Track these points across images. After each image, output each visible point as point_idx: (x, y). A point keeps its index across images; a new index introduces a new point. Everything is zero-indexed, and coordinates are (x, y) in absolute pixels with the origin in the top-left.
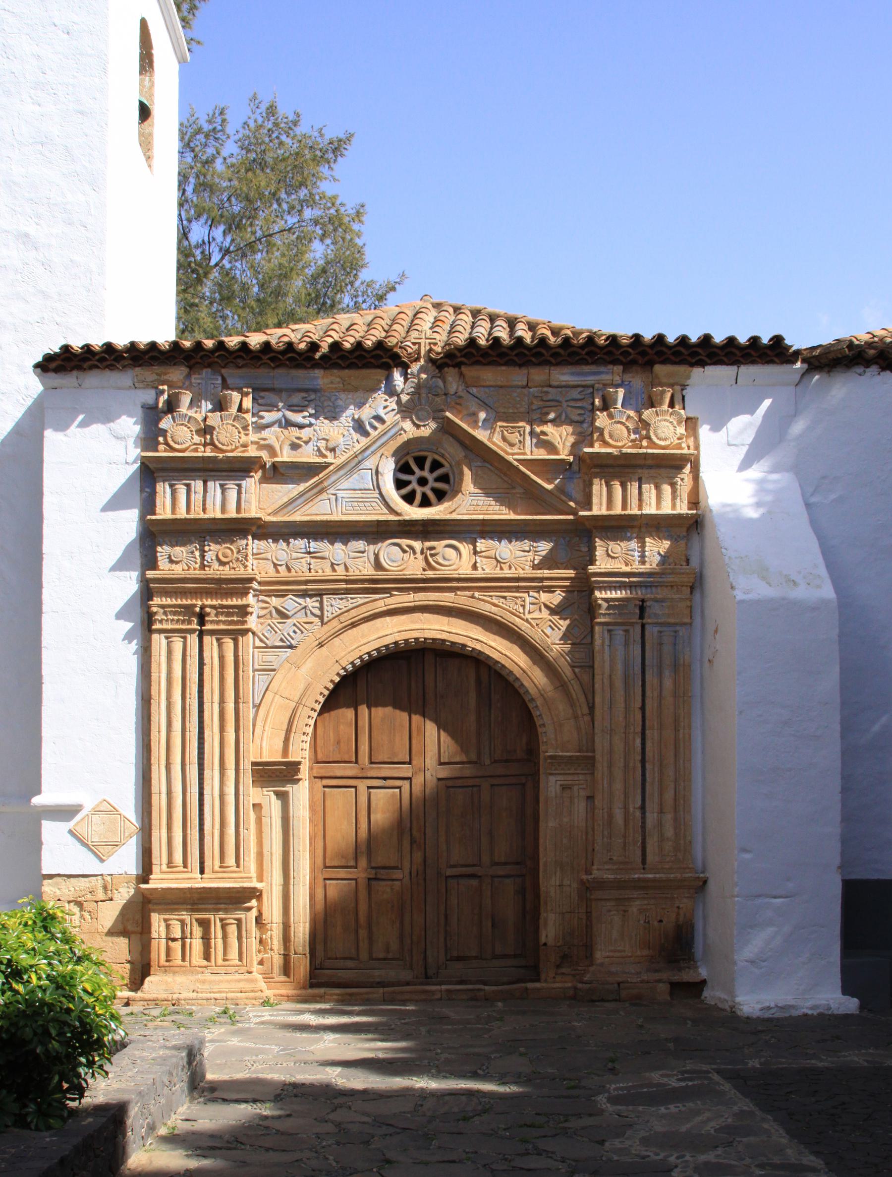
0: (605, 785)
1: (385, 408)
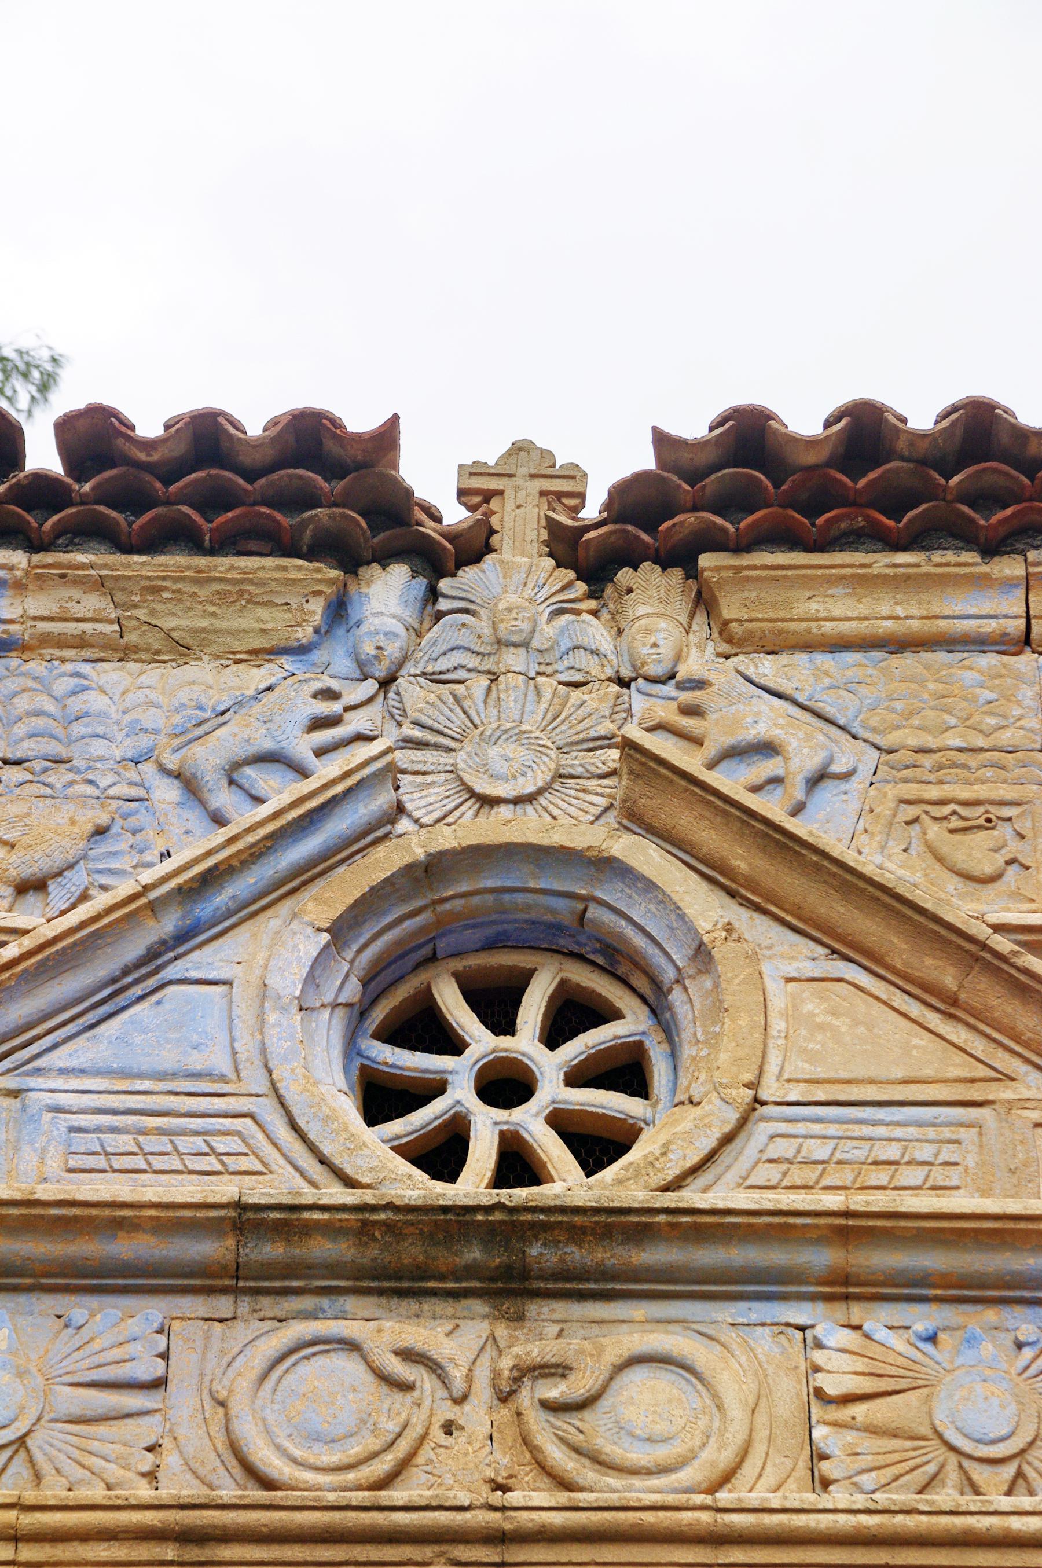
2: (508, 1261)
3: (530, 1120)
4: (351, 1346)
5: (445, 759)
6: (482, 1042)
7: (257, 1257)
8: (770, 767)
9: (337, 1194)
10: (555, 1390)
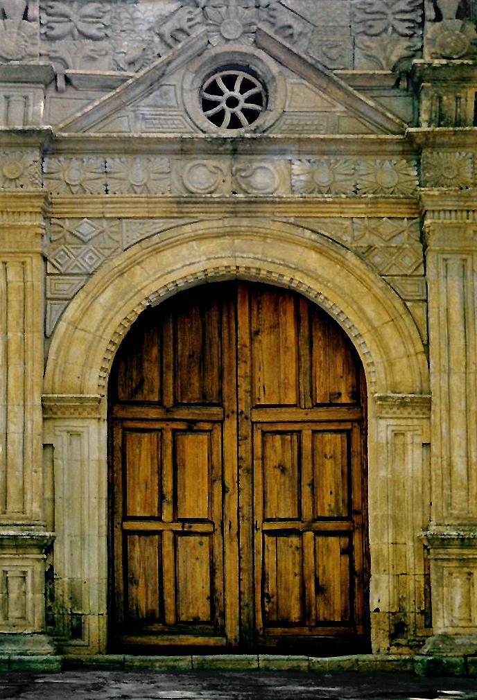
0: (444, 430)
1: (189, 20)
2: (234, 149)
3: (237, 110)
4: (205, 166)
5: (218, 28)
6: (228, 93)
7: (184, 148)
8: (290, 31)
9: (202, 135)
10: (243, 174)
